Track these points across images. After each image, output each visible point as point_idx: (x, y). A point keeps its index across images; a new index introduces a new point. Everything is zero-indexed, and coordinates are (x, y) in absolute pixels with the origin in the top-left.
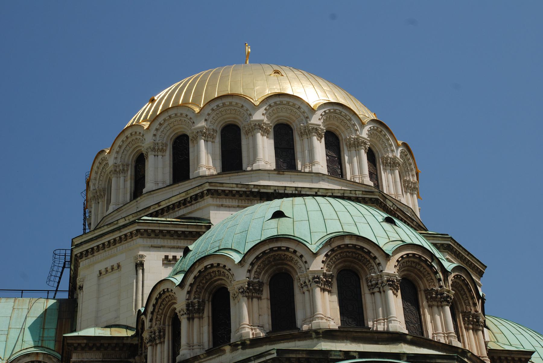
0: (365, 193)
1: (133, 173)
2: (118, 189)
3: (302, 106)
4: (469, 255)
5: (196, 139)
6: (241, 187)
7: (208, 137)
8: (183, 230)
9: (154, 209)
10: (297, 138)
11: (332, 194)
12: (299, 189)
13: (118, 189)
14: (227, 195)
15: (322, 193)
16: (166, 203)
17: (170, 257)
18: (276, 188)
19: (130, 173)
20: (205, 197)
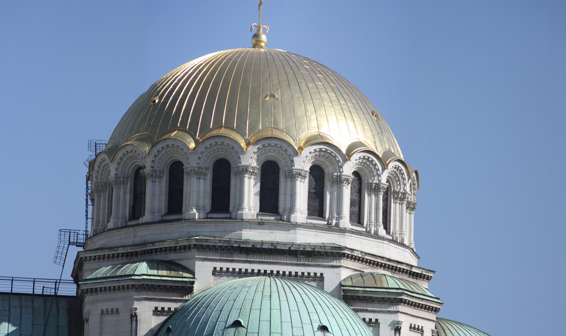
0: (334, 248)
1: (133, 186)
2: (118, 201)
3: (288, 149)
4: (424, 300)
5: (189, 174)
6: (224, 243)
7: (200, 175)
8: (171, 284)
9: (149, 246)
10: (282, 179)
11: (304, 249)
12: (275, 245)
13: (118, 201)
14: (210, 249)
15: (295, 248)
16: (159, 245)
17: (159, 309)
18: (255, 244)
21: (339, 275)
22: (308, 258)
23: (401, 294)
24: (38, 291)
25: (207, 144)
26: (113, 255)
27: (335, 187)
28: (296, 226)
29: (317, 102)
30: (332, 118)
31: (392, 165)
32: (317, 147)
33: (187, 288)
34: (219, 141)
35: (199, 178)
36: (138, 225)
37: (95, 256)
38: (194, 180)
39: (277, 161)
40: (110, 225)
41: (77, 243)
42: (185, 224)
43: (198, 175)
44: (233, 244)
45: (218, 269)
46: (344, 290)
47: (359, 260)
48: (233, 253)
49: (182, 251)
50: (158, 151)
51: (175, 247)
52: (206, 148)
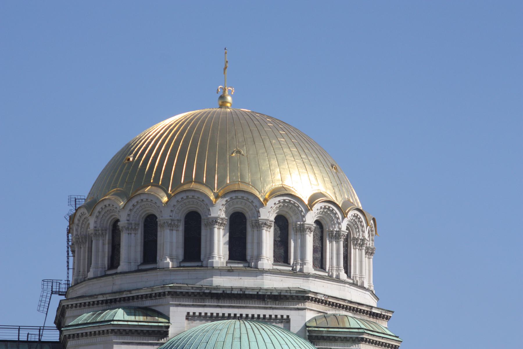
0: (299, 292)
1: (111, 238)
2: (97, 251)
3: (254, 201)
4: (384, 338)
5: (162, 226)
6: (196, 289)
7: (173, 227)
8: (148, 329)
9: (126, 294)
11: (271, 294)
12: (243, 290)
13: (97, 251)
14: (184, 295)
15: (262, 292)
16: (136, 293)
18: (225, 290)
19: (108, 237)
20: (167, 296)
21: (304, 317)
22: (275, 302)
23: (363, 333)
24: (23, 338)
25: (179, 198)
26: (94, 302)
27: (299, 235)
28: (263, 272)
29: (280, 157)
30: (295, 171)
31: (351, 214)
32: (281, 199)
33: (163, 333)
34: (190, 195)
35: (172, 230)
36: (116, 274)
37: (76, 304)
38: (167, 232)
39: (244, 212)
40: (90, 275)
41: (59, 292)
42: (159, 273)
43: (171, 227)
44: (204, 290)
45: (191, 314)
46: (309, 331)
47: (322, 303)
48: (205, 298)
49: (157, 298)
50: (134, 205)
51: (151, 294)
52: (178, 201)
